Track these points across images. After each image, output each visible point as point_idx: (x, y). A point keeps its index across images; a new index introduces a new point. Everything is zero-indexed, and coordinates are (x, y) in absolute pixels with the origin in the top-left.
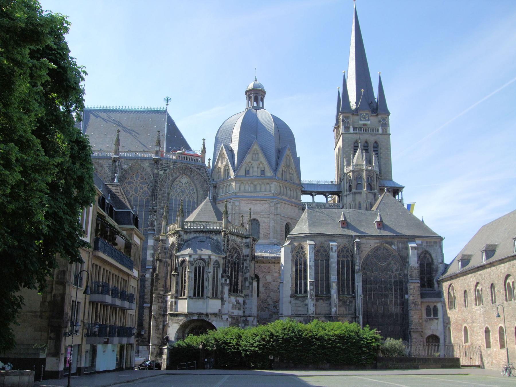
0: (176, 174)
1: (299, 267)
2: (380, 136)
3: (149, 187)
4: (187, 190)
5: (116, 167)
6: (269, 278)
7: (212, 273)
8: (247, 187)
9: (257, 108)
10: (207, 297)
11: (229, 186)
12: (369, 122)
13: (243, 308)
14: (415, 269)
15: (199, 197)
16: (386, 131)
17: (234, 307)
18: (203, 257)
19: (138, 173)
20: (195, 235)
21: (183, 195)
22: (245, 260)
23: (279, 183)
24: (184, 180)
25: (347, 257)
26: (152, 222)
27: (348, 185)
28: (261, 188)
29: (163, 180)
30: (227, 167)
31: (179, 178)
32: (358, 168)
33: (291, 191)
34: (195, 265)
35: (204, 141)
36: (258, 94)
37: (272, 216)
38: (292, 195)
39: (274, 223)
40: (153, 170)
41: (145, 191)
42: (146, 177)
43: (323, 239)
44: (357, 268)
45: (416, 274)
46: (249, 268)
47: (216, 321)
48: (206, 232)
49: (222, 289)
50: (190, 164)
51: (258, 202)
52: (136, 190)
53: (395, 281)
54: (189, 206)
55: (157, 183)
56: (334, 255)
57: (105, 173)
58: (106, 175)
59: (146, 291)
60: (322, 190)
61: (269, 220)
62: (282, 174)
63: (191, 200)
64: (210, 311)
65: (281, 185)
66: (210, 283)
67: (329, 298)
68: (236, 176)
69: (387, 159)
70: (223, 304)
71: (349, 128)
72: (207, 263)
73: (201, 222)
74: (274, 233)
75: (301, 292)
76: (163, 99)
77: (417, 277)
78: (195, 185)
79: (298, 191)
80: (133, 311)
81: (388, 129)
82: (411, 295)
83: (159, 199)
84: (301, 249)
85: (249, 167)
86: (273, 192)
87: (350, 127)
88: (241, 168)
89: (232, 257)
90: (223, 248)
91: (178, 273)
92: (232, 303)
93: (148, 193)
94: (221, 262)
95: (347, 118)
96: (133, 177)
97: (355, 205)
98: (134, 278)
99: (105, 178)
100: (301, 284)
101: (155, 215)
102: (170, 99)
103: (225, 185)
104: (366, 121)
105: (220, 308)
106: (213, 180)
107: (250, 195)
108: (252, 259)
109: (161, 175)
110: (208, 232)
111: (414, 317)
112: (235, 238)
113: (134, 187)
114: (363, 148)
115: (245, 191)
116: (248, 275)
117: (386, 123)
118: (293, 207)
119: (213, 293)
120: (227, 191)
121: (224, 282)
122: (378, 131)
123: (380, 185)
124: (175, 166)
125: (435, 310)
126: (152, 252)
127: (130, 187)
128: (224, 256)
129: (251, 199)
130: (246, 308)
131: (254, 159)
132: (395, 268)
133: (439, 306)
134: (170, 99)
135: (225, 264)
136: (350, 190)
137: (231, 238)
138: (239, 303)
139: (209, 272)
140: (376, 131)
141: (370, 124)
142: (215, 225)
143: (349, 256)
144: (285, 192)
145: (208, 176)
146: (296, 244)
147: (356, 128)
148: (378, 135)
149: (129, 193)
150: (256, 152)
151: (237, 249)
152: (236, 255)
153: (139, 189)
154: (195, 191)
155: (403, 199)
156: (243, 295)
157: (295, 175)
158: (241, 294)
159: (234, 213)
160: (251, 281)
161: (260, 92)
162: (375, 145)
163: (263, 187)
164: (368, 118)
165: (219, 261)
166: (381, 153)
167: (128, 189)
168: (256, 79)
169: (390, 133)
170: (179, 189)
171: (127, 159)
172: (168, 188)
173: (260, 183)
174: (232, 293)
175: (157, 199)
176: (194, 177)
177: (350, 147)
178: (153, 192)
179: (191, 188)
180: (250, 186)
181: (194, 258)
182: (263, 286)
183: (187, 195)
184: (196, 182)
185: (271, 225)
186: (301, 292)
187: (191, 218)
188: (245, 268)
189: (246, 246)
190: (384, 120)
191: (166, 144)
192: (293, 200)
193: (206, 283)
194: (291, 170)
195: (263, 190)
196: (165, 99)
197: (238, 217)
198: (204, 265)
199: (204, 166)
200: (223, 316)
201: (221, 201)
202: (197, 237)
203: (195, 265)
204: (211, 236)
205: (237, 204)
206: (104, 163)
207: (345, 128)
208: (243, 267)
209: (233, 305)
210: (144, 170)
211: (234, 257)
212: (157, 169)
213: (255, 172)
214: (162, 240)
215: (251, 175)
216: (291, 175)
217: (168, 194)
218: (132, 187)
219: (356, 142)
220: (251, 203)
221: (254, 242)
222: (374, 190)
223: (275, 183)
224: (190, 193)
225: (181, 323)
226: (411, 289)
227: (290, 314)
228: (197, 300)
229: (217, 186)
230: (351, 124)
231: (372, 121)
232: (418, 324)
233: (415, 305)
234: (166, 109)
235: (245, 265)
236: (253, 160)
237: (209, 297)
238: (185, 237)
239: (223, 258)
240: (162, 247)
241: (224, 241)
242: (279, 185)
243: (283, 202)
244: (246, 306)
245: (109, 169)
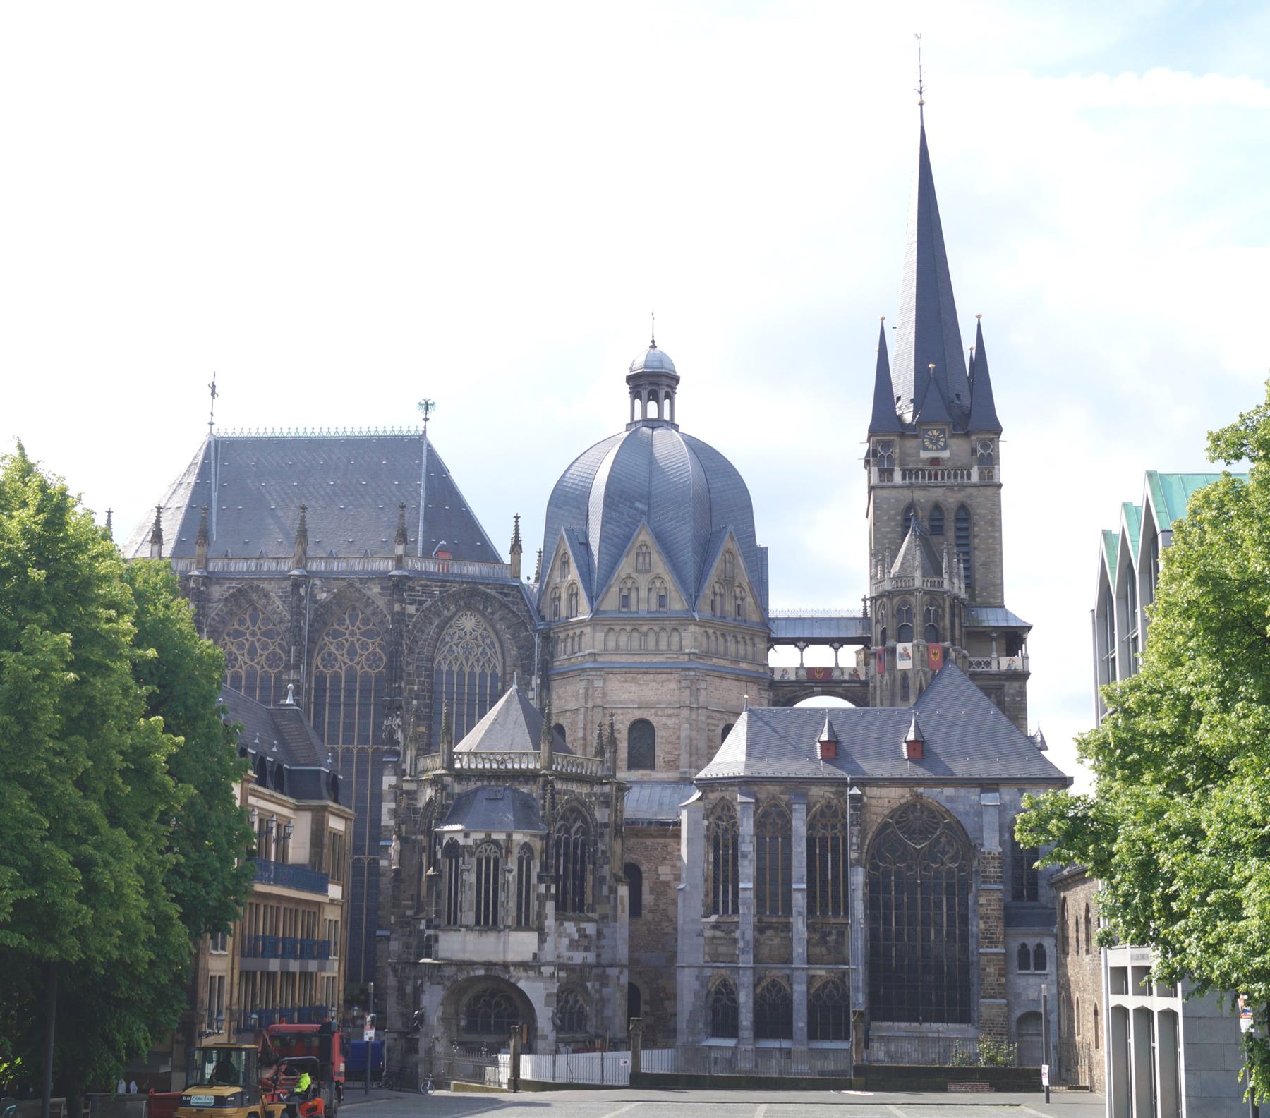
0: (448, 610)
1: (721, 852)
2: (974, 491)
3: (383, 643)
4: (478, 646)
5: (301, 599)
6: (665, 872)
7: (515, 872)
8: (623, 639)
9: (655, 424)
10: (506, 927)
11: (580, 636)
12: (945, 454)
13: (597, 947)
14: (993, 858)
15: (507, 664)
16: (991, 477)
17: (573, 945)
18: (494, 836)
19: (354, 609)
20: (479, 784)
21: (467, 660)
22: (602, 835)
23: (705, 626)
24: (469, 622)
25: (834, 827)
26: (392, 732)
27: (880, 628)
28: (657, 644)
29: (414, 627)
30: (574, 587)
31: (456, 618)
32: (904, 585)
33: (737, 642)
34: (477, 855)
35: (517, 522)
36: (658, 385)
37: (685, 713)
38: (742, 652)
39: (691, 730)
40: (390, 604)
41: (374, 654)
42: (376, 619)
43: (777, 788)
44: (853, 855)
45: (993, 869)
46: (608, 854)
47: (528, 978)
48: (504, 777)
49: (540, 906)
50: (481, 584)
51: (652, 676)
52: (352, 653)
53: (948, 885)
54: (483, 686)
55: (402, 637)
56: (799, 826)
57: (275, 612)
58: (276, 618)
59: (381, 899)
60: (825, 634)
61: (677, 721)
62: (713, 602)
63: (489, 672)
64: (512, 957)
65: (711, 631)
66: (510, 894)
67: (788, 927)
68: (595, 612)
70: (542, 940)
71: (891, 472)
72: (504, 851)
73: (492, 753)
74: (691, 755)
75: (725, 911)
76: (416, 405)
77: (998, 877)
78: (496, 632)
79: (757, 640)
80: (334, 968)
81: (996, 471)
82: (982, 918)
83: (409, 674)
84: (725, 812)
85: (629, 589)
86: (687, 651)
87: (893, 470)
88: (606, 593)
89: (567, 831)
90: (541, 813)
91: (441, 871)
92: (569, 936)
93: (381, 659)
94: (538, 845)
95: (887, 445)
96: (344, 619)
97: (894, 680)
98: (332, 902)
99: (274, 625)
100: (725, 892)
101: (398, 716)
102: (433, 405)
103: (571, 633)
104: (937, 449)
105: (536, 950)
106: (543, 618)
107: (630, 659)
108: (616, 834)
109: (411, 616)
110: (509, 777)
111: (988, 970)
112: (575, 787)
113: (347, 645)
114: (926, 524)
115: (617, 649)
116: (606, 870)
117: (990, 454)
119: (519, 916)
120: (576, 649)
121: (544, 891)
122: (969, 476)
123: (967, 624)
124: (445, 592)
125: (1040, 949)
126: (393, 805)
127: (337, 644)
128: (544, 832)
129: (632, 671)
130: (603, 947)
131: (640, 567)
132: (952, 853)
133: (1048, 943)
134: (433, 405)
135: (545, 851)
136: (884, 643)
137: (564, 787)
138: (586, 936)
139: (510, 871)
140: (962, 477)
141: (948, 459)
142: (524, 759)
143: (839, 825)
144: (721, 648)
145: (528, 611)
146: (714, 796)
147: (910, 471)
148: (969, 490)
149: (336, 659)
150: (644, 549)
151: (580, 812)
152: (577, 825)
153: (359, 651)
154: (498, 650)
155: (1028, 658)
156: (595, 916)
157: (750, 600)
158: (590, 915)
159: (590, 705)
160: (613, 883)
161: (663, 379)
162: (962, 515)
163: (664, 637)
164: (945, 442)
165: (532, 844)
166: (975, 536)
167: (333, 649)
168: (653, 342)
170: (457, 645)
171: (327, 577)
172: (429, 645)
173: (656, 629)
174: (569, 914)
175: (401, 678)
176: (492, 613)
178: (390, 661)
179: (488, 641)
180: (630, 637)
181: (475, 840)
182: (652, 891)
183: (478, 660)
184: (498, 626)
185: (683, 735)
186: (725, 911)
187: (468, 743)
188: (600, 854)
189: (603, 802)
190: (985, 446)
191: (424, 532)
192: (744, 666)
193: (502, 896)
194: (738, 590)
195: (663, 646)
196: (419, 404)
197: (600, 716)
198: (499, 855)
199: (519, 589)
200: (543, 969)
201: (563, 674)
202: (483, 788)
203: (477, 855)
204: (517, 783)
205: (598, 684)
206: (273, 589)
207: (881, 472)
208: (596, 852)
209: (572, 941)
210: (369, 602)
211: (573, 831)
212: (402, 601)
213: (643, 602)
214: (408, 792)
215: (633, 608)
216: (739, 602)
217: (432, 660)
218: (343, 644)
219: (911, 507)
220: (634, 680)
221: (620, 794)
222: (944, 641)
223: (692, 628)
224: (484, 653)
225: (448, 984)
226: (981, 905)
227: (701, 962)
228: (484, 935)
229: (552, 635)
230: (897, 462)
231: (951, 451)
232: (996, 987)
233: (989, 942)
234: (425, 432)
235: (601, 847)
236: (637, 571)
237: (509, 927)
238: (457, 788)
239: (542, 838)
240: (409, 809)
241: (544, 798)
242: (706, 632)
243: (716, 674)
244: (603, 942)
245: (284, 602)
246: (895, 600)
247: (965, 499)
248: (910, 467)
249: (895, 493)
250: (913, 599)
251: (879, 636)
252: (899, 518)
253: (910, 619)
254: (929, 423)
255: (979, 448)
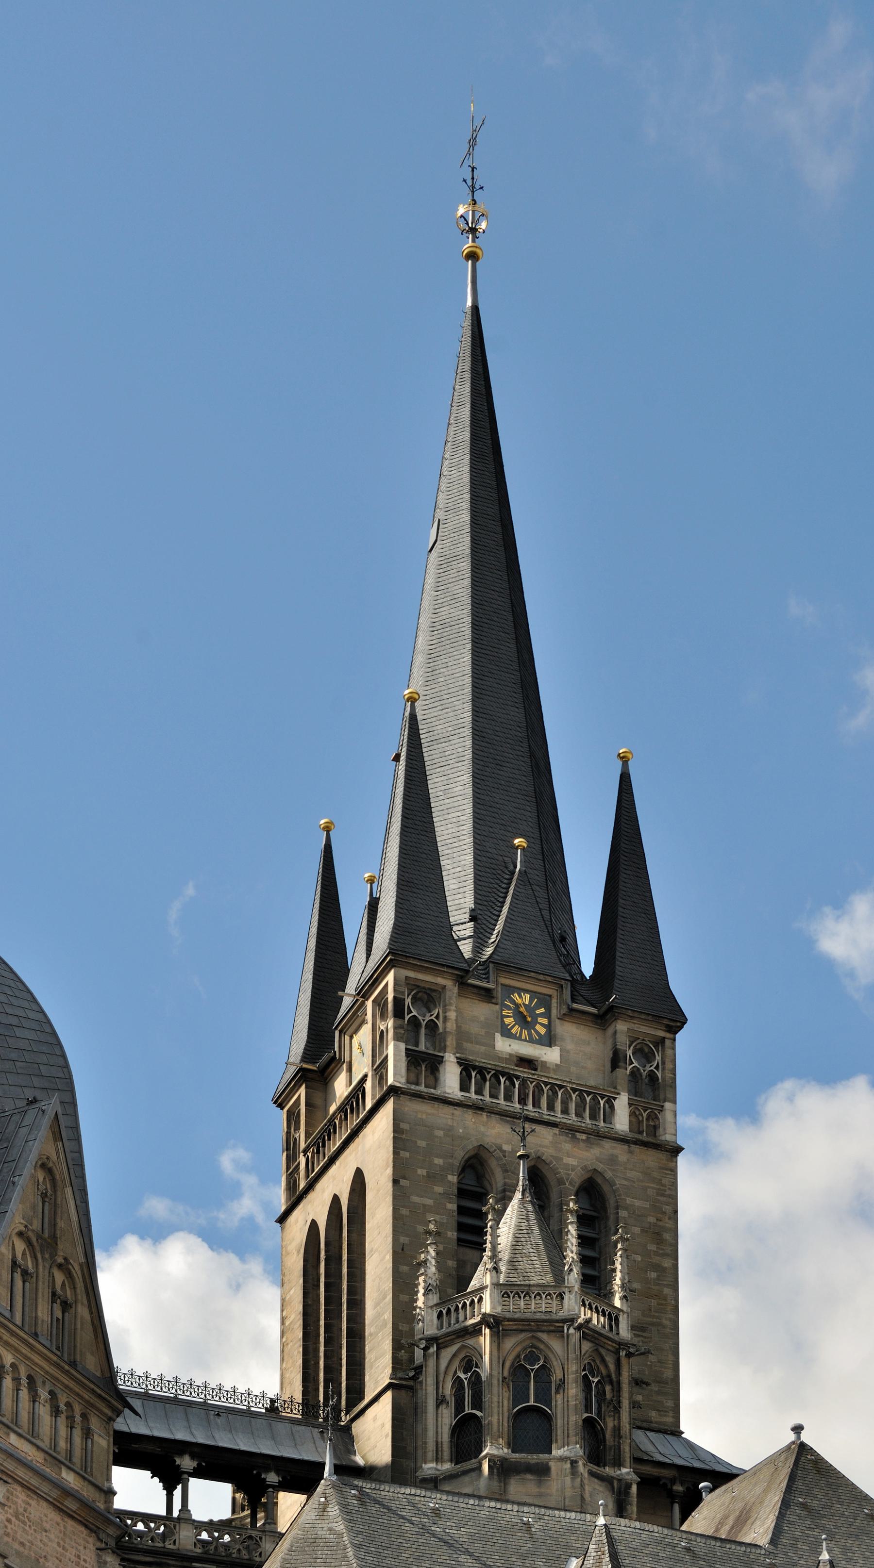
2: (620, 1151)
12: (551, 1055)
69: (654, 1303)
81: (668, 1116)
104: (531, 1041)
118: (70, 1523)
122: (609, 1116)
148: (608, 1145)
157: (83, 1311)
164: (549, 1027)
169: (680, 1142)
177: (439, 1189)
192: (69, 1478)
222: (618, 1463)
246: (509, 1343)
247: (600, 1167)
248: (481, 1060)
249: (444, 1116)
250: (556, 1345)
251: (446, 1437)
252: (453, 1179)
253: (544, 1395)
254: (518, 970)
255: (629, 1053)
